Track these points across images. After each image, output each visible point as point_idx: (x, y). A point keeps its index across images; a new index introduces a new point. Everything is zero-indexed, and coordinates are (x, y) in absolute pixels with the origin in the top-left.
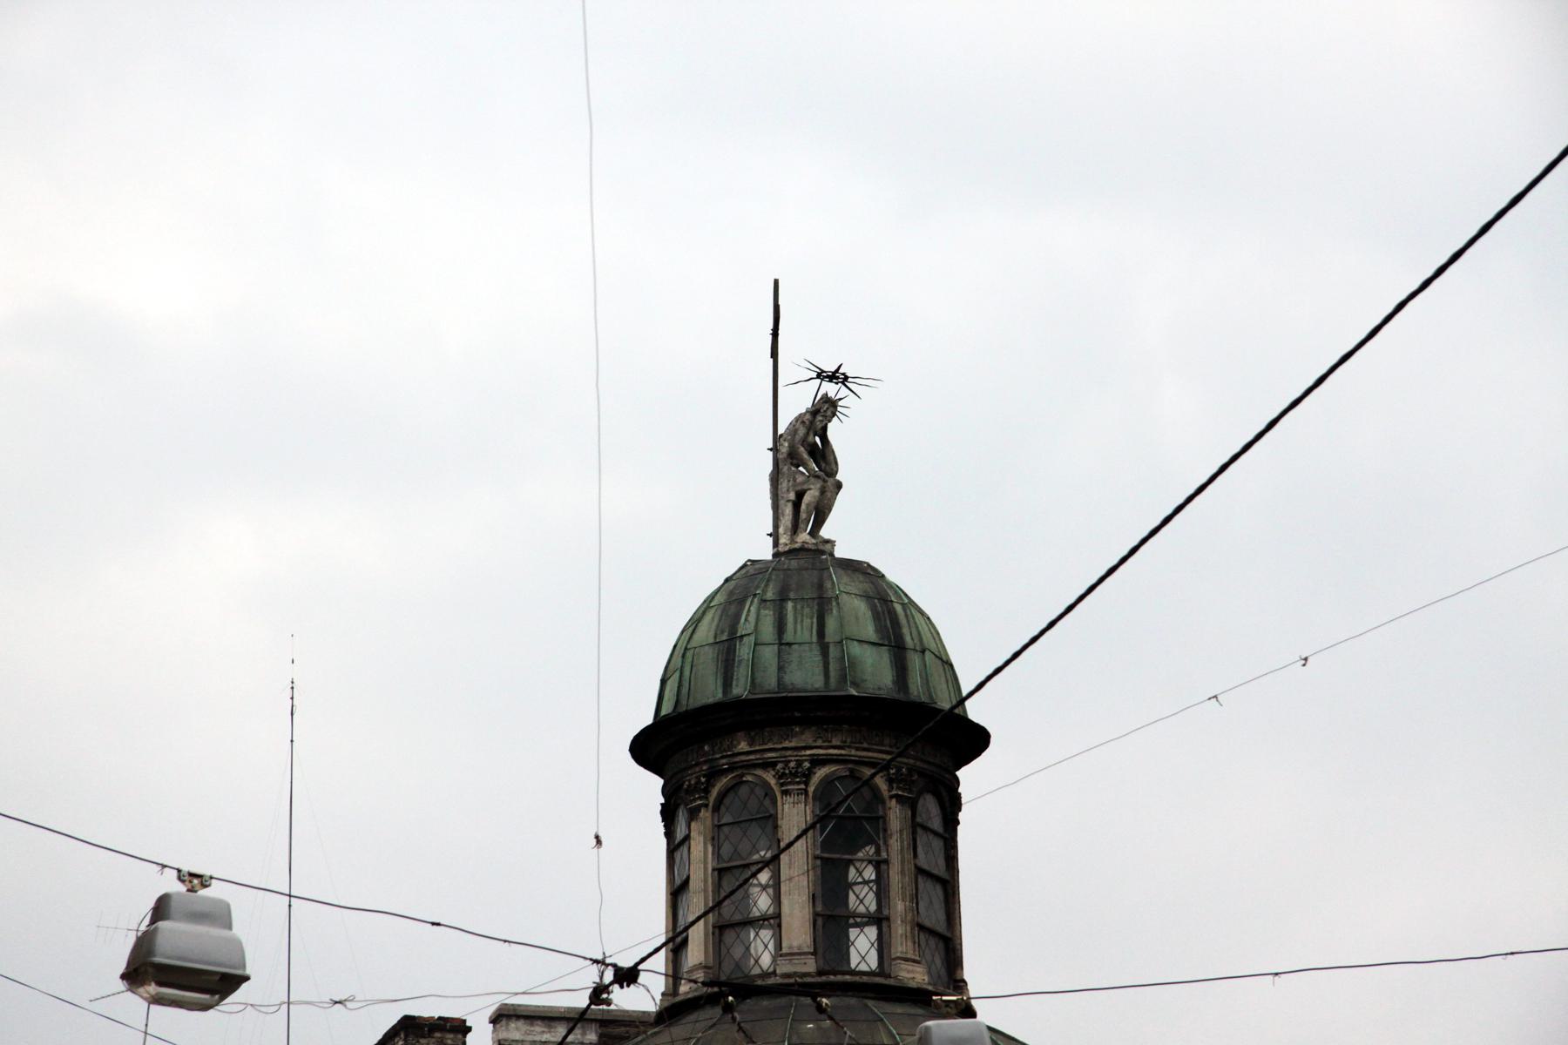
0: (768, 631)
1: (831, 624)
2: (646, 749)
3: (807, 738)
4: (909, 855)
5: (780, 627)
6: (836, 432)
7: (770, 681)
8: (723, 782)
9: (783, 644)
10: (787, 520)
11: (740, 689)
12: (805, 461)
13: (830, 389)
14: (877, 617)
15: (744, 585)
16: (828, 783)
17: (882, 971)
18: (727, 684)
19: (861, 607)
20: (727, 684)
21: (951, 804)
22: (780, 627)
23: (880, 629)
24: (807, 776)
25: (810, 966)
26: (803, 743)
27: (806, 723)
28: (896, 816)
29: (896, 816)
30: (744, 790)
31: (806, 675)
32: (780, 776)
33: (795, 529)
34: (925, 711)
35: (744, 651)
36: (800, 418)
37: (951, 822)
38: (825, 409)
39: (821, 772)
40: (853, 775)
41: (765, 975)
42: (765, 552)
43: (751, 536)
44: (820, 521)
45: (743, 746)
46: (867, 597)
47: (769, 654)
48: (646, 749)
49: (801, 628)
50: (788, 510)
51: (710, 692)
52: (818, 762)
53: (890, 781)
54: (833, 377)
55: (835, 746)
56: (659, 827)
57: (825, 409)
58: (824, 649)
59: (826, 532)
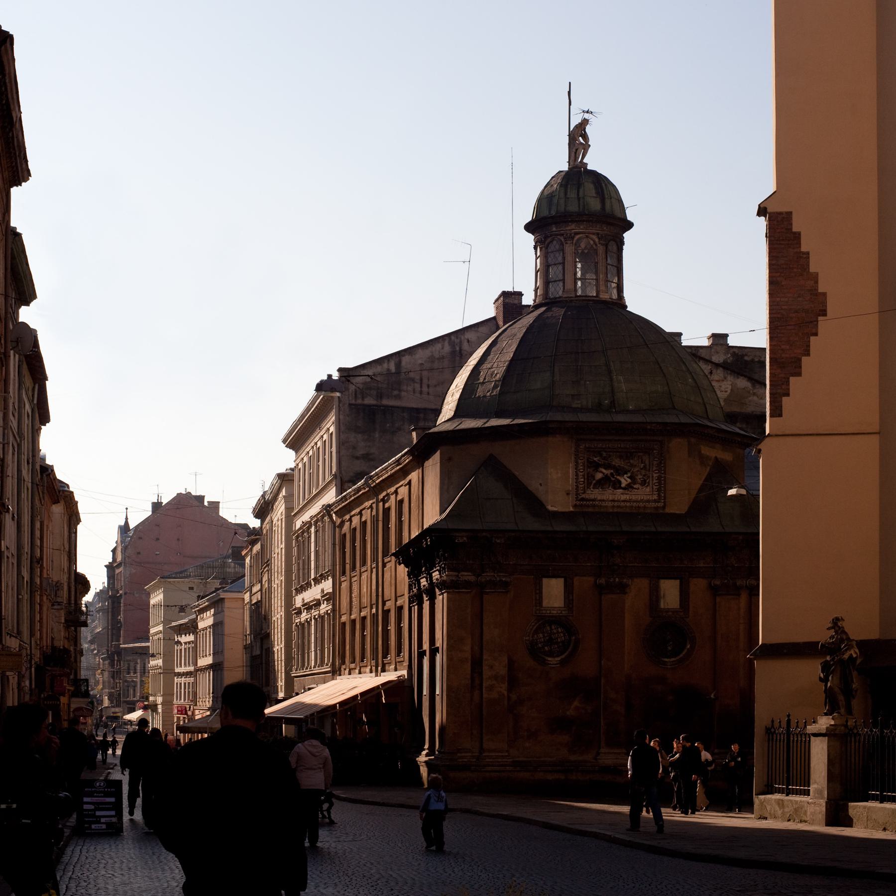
0: (562, 195)
1: (581, 191)
2: (529, 227)
3: (573, 226)
4: (604, 260)
5: (566, 194)
6: (589, 129)
8: (549, 240)
9: (566, 198)
10: (572, 158)
13: (587, 116)
14: (596, 188)
16: (578, 239)
17: (597, 296)
18: (550, 210)
19: (592, 186)
20: (550, 210)
21: (620, 243)
22: (566, 194)
23: (597, 193)
24: (573, 238)
25: (573, 295)
26: (572, 227)
27: (572, 221)
28: (601, 249)
30: (555, 242)
31: (573, 207)
33: (576, 158)
34: (612, 216)
35: (555, 200)
36: (576, 126)
37: (620, 250)
38: (585, 122)
39: (577, 237)
41: (560, 297)
42: (565, 167)
45: (554, 229)
46: (594, 183)
47: (562, 202)
48: (529, 227)
49: (572, 194)
50: (573, 154)
51: (545, 213)
52: (576, 234)
54: (587, 112)
55: (581, 228)
56: (533, 251)
57: (585, 122)
58: (579, 199)
59: (585, 161)
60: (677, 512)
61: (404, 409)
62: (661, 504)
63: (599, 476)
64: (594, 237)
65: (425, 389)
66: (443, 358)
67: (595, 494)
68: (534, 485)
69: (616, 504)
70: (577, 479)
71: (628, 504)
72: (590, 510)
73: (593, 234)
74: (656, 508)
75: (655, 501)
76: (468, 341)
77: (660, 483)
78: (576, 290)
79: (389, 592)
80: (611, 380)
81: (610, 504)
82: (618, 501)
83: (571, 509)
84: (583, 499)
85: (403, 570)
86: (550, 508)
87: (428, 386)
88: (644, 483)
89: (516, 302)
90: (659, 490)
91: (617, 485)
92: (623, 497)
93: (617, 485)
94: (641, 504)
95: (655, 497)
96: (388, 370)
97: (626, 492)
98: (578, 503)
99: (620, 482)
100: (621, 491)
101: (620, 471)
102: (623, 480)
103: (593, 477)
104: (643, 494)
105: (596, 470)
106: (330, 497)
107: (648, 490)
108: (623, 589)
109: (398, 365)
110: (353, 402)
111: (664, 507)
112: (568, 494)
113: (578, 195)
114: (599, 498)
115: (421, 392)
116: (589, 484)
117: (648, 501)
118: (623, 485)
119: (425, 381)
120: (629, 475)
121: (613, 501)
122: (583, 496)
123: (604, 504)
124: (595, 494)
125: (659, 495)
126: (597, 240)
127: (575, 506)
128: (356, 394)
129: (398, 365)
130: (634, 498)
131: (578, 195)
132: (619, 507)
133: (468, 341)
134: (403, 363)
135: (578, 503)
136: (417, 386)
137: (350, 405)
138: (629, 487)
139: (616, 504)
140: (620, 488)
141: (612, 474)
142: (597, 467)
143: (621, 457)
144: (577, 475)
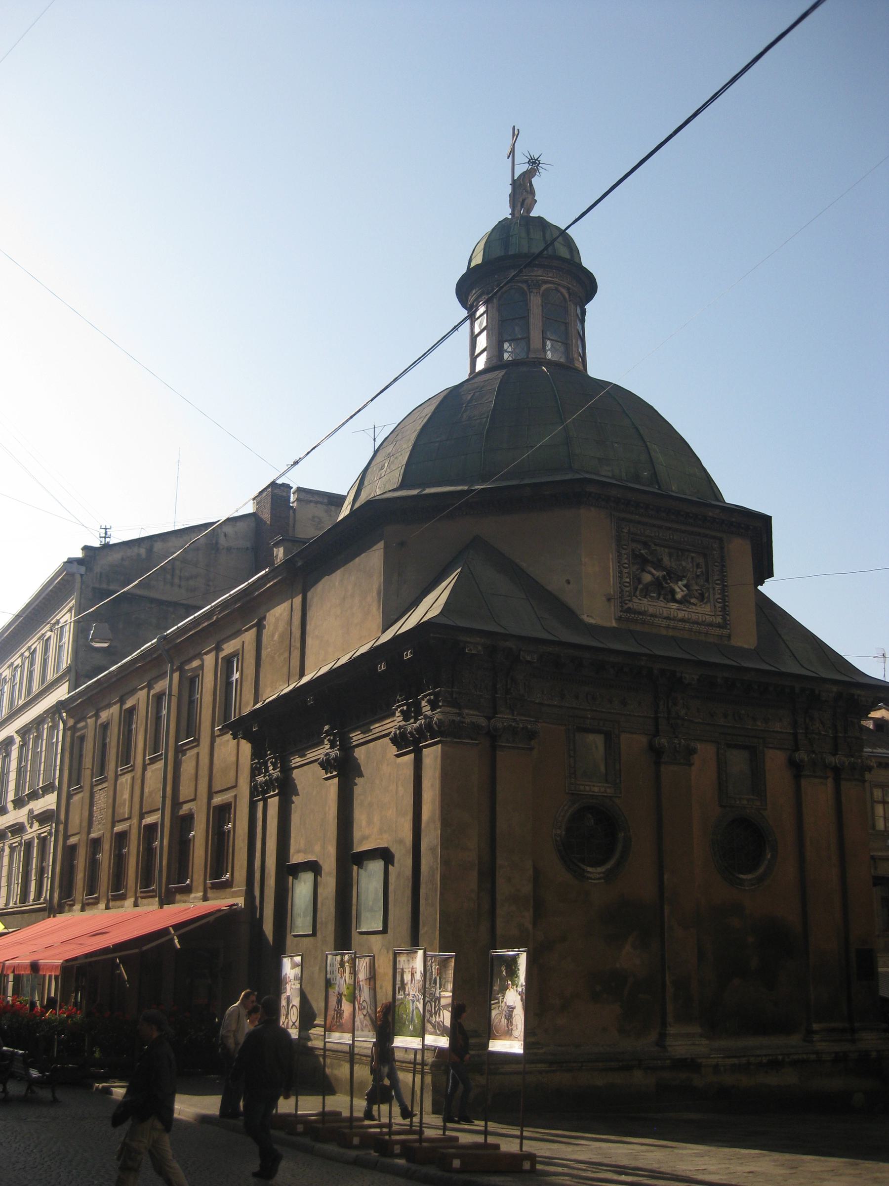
3: (540, 272)
5: (528, 233)
7: (525, 250)
11: (511, 252)
12: (522, 190)
15: (502, 231)
16: (546, 290)
21: (584, 312)
22: (528, 233)
24: (539, 286)
26: (538, 273)
29: (571, 306)
32: (529, 286)
39: (545, 287)
40: (556, 289)
43: (505, 212)
44: (529, 210)
53: (570, 294)
60: (746, 646)
61: (152, 600)
62: (725, 632)
63: (647, 578)
64: (564, 291)
65: (177, 581)
66: (198, 549)
67: (643, 604)
68: (554, 583)
69: (672, 623)
70: (621, 577)
71: (687, 626)
72: (638, 628)
73: (564, 287)
74: (721, 637)
75: (719, 626)
76: (225, 535)
77: (724, 601)
78: (545, 351)
79: (185, 791)
80: (647, 446)
81: (665, 623)
82: (674, 619)
83: (614, 624)
84: (629, 610)
85: (246, 747)
86: (585, 618)
87: (180, 578)
88: (702, 598)
89: (284, 494)
90: (724, 608)
91: (671, 596)
92: (681, 615)
93: (671, 596)
94: (703, 629)
95: (719, 620)
96: (139, 555)
97: (682, 607)
98: (624, 615)
99: (673, 592)
100: (675, 606)
101: (673, 575)
102: (678, 590)
103: (639, 581)
104: (703, 612)
105: (643, 570)
106: (62, 693)
107: (707, 609)
108: (692, 752)
109: (150, 551)
110: (97, 585)
111: (729, 637)
112: (609, 600)
113: (544, 236)
114: (651, 610)
115: (172, 584)
116: (636, 589)
117: (711, 625)
118: (679, 596)
119: (177, 572)
120: (685, 582)
121: (668, 618)
122: (630, 605)
123: (657, 621)
124: (643, 604)
125: (724, 619)
126: (567, 296)
127: (619, 620)
128: (101, 576)
129: (150, 551)
130: (694, 617)
131: (544, 236)
132: (674, 628)
133: (225, 535)
134: (155, 549)
135: (624, 615)
136: (169, 577)
137: (94, 589)
138: (684, 601)
139: (672, 623)
140: (674, 600)
141: (664, 577)
142: (642, 562)
143: (670, 555)
144: (621, 572)
